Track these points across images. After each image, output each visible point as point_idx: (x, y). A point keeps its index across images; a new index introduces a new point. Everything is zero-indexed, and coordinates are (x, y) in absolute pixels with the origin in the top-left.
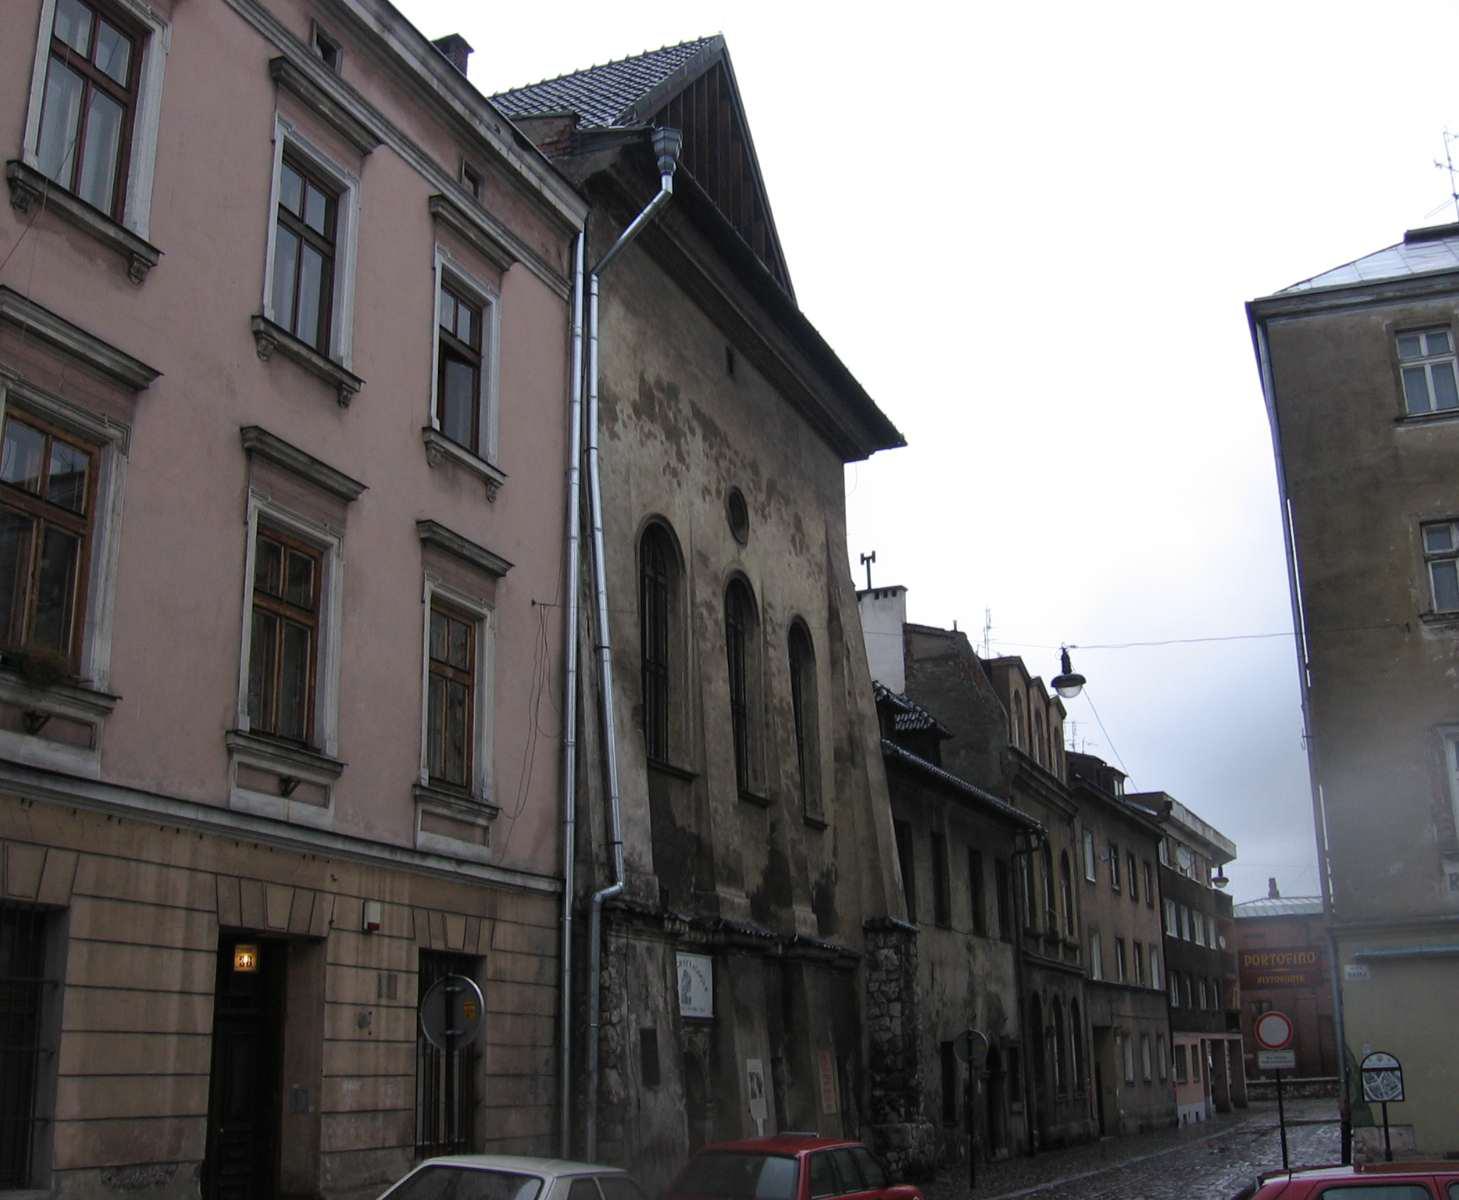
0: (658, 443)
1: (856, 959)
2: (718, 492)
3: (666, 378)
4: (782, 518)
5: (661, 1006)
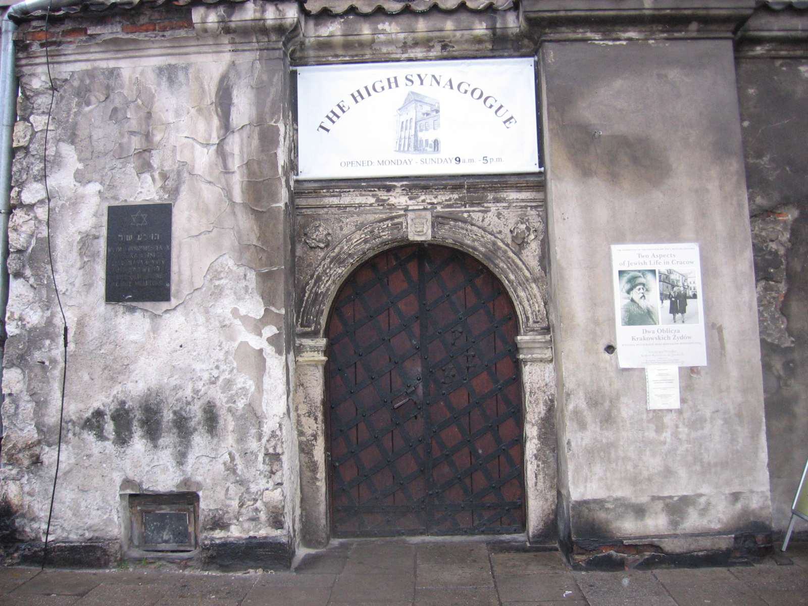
5: (203, 159)
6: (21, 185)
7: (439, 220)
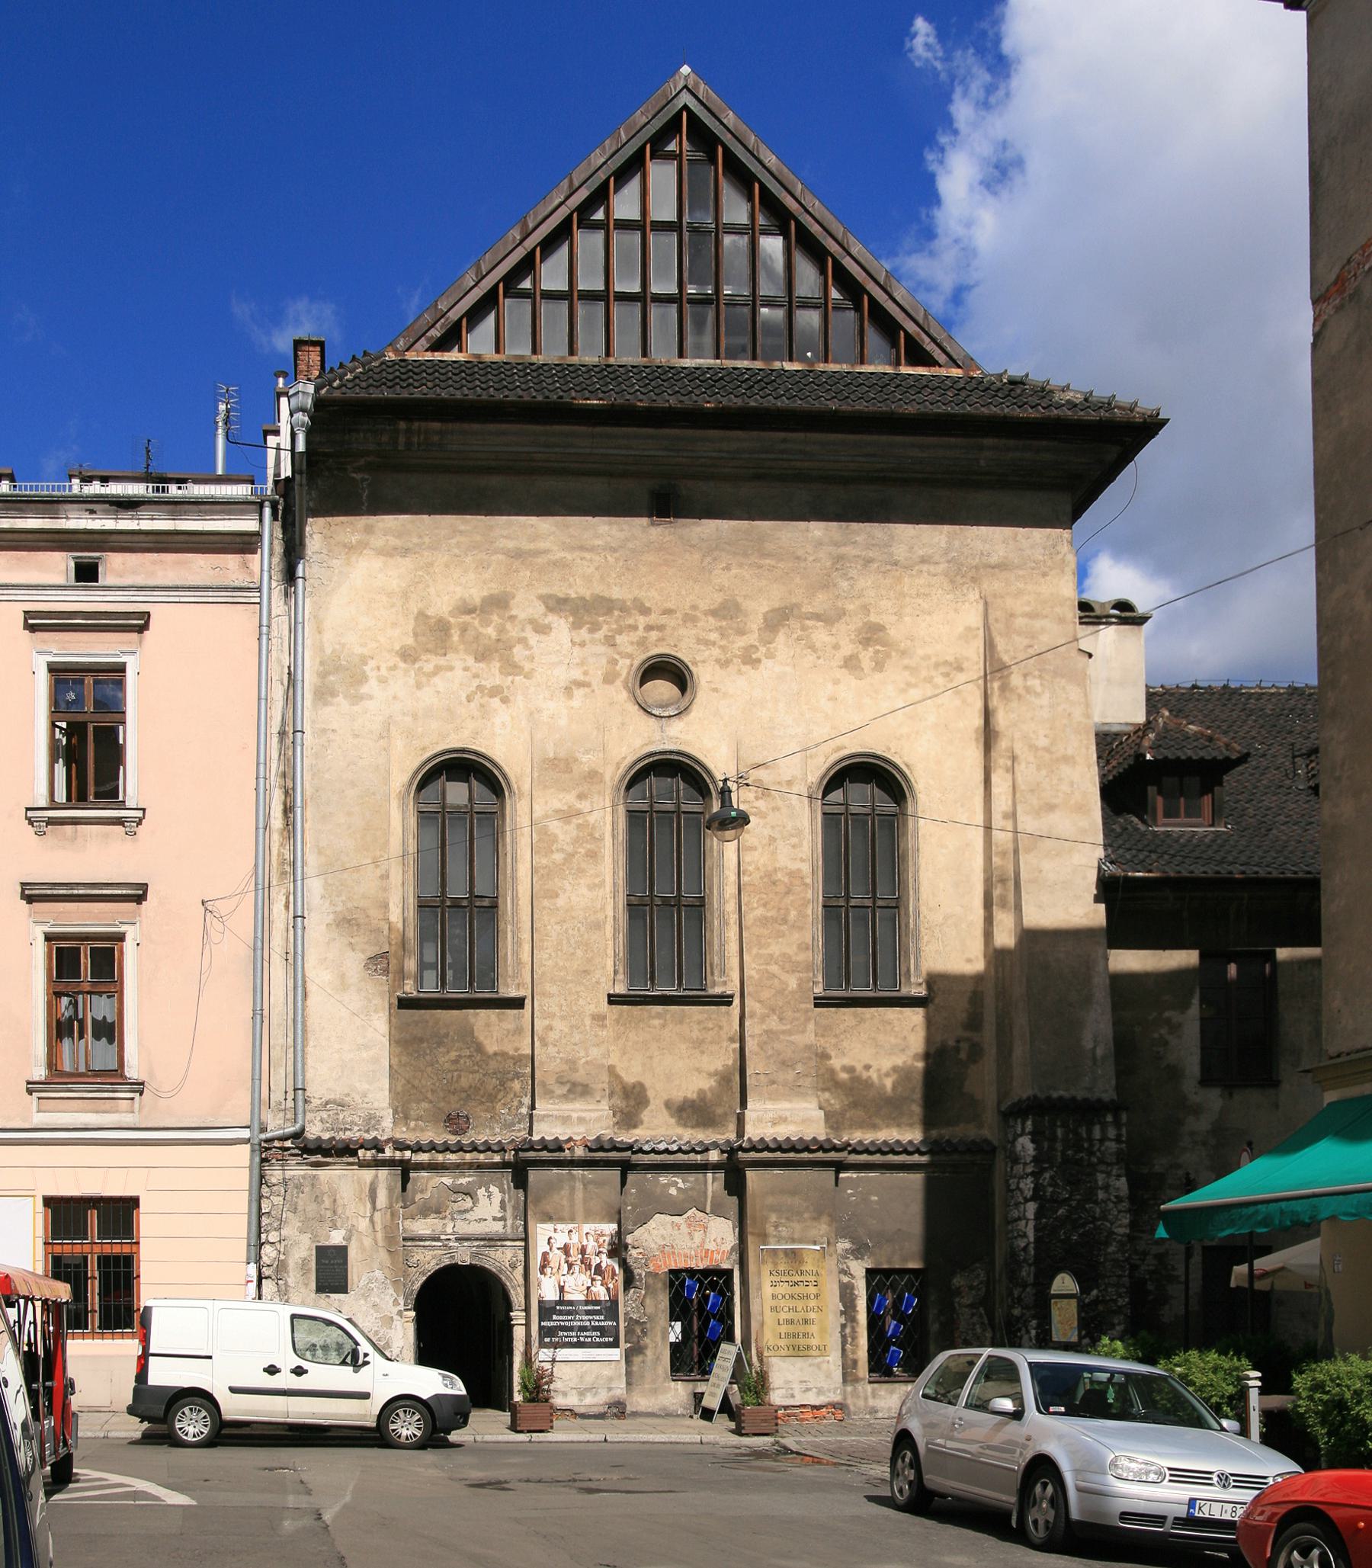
0: (459, 673)
1: (994, 1150)
2: (609, 679)
3: (476, 594)
4: (813, 648)
5: (363, 1224)
6: (267, 1232)
7: (473, 1255)
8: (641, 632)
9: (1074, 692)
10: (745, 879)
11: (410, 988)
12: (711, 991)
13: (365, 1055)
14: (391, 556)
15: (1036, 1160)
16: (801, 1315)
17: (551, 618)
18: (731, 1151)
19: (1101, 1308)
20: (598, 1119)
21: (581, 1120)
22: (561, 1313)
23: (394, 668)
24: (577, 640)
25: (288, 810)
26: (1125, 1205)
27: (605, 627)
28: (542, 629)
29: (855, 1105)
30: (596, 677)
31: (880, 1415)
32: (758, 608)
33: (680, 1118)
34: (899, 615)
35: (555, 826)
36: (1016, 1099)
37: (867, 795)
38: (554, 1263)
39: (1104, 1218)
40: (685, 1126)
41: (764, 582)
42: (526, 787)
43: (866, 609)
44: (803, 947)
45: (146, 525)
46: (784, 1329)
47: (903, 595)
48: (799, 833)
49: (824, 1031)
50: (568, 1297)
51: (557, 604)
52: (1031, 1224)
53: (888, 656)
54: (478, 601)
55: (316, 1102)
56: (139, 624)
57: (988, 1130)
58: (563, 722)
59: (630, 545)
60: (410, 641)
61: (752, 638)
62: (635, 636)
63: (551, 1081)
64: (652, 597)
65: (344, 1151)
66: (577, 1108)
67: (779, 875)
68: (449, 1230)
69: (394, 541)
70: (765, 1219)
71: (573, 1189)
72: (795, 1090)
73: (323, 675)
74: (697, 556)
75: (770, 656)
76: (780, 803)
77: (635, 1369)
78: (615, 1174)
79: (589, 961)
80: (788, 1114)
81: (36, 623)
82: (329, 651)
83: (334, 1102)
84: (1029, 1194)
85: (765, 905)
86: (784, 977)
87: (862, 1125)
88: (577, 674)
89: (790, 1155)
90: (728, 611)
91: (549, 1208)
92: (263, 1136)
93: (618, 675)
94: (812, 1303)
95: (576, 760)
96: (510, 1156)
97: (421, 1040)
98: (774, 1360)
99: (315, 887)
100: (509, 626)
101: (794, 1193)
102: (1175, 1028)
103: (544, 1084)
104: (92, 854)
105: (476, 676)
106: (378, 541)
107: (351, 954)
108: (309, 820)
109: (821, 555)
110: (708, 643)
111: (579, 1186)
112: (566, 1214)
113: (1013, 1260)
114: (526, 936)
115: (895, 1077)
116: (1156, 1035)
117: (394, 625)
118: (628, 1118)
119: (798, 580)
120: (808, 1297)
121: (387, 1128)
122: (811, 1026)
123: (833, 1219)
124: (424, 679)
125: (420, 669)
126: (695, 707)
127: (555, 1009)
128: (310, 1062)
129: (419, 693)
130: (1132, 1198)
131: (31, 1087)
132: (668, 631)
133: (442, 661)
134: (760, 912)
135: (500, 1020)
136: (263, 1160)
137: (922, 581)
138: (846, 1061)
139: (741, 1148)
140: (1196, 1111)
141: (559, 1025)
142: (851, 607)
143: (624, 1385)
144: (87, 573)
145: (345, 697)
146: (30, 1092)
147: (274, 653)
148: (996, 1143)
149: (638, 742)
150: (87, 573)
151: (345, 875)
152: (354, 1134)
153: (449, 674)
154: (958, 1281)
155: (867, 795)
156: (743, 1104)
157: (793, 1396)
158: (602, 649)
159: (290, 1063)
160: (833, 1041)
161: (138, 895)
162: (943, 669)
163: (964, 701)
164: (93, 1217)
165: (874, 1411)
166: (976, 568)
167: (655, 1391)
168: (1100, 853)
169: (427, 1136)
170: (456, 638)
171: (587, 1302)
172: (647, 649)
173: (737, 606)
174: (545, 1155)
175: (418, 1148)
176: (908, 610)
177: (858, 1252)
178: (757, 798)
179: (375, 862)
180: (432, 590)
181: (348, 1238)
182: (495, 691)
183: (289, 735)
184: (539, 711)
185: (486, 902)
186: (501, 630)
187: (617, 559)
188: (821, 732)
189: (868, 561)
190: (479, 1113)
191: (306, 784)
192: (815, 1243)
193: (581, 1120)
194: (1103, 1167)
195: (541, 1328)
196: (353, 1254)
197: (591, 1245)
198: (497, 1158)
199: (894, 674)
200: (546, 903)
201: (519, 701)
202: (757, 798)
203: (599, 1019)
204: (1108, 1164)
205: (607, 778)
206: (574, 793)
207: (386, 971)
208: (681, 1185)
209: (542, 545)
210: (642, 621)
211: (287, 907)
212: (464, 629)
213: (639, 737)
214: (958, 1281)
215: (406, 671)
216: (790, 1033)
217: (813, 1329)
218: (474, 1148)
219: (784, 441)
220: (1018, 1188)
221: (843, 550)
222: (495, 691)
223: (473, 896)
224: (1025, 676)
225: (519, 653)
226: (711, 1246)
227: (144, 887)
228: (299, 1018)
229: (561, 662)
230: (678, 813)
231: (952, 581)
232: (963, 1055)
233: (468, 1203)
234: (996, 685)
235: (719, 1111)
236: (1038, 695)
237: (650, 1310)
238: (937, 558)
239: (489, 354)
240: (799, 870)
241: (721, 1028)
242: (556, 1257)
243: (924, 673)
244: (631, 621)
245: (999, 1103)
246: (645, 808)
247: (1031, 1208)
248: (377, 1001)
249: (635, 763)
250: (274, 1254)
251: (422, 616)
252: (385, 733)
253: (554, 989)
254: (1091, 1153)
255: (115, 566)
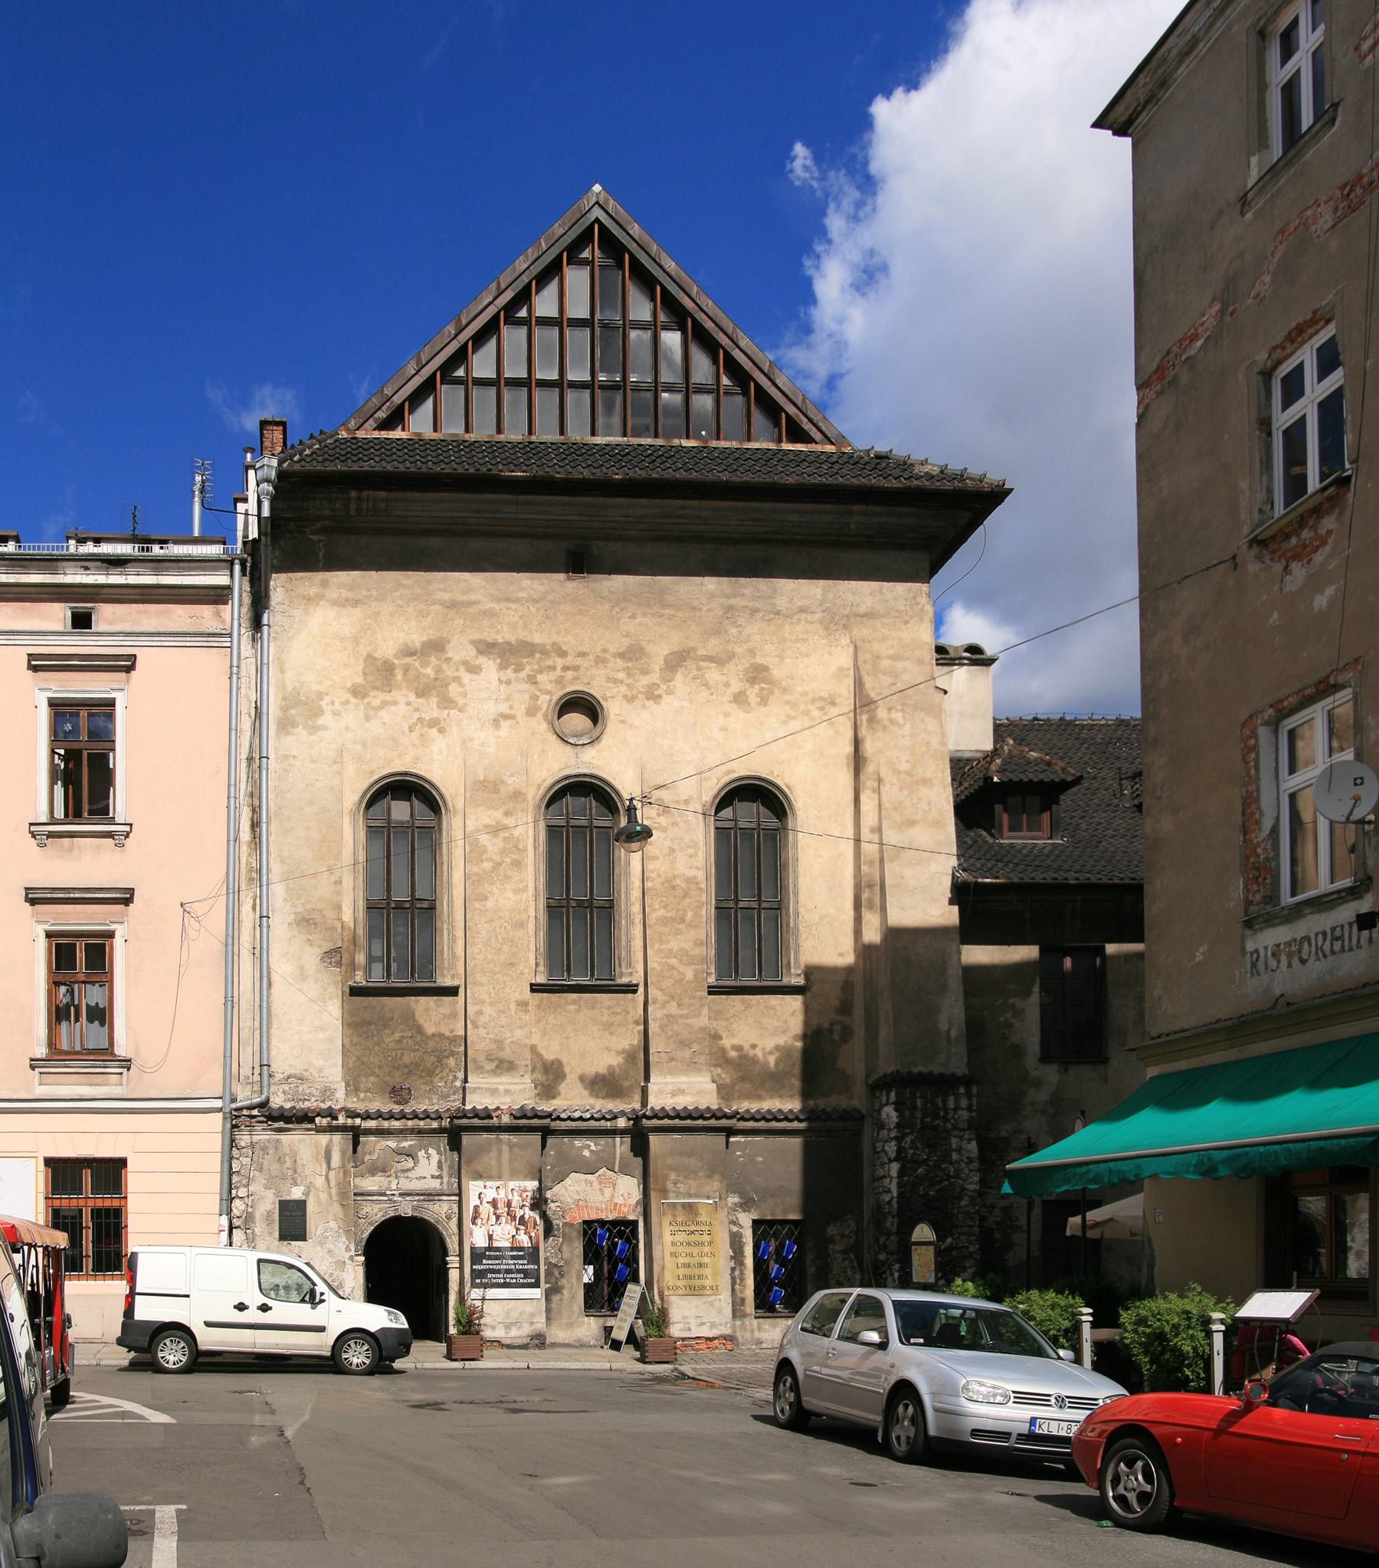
0: (402, 707)
1: (862, 1118)
2: (531, 712)
3: (417, 639)
4: (706, 685)
5: (320, 1181)
7: (414, 1208)
8: (559, 672)
9: (931, 724)
10: (648, 884)
11: (359, 978)
12: (619, 981)
13: (321, 1036)
14: (344, 606)
15: (898, 1126)
16: (697, 1259)
17: (482, 660)
18: (636, 1119)
19: (954, 1253)
20: (522, 1091)
21: (507, 1092)
22: (490, 1258)
23: (346, 703)
24: (504, 679)
25: (255, 825)
26: (976, 1165)
27: (528, 668)
28: (474, 670)
29: (743, 1079)
30: (520, 710)
31: (764, 1345)
32: (659, 652)
33: (592, 1090)
34: (781, 657)
35: (484, 839)
36: (882, 1073)
37: (754, 813)
38: (484, 1215)
39: (957, 1176)
40: (597, 1097)
41: (665, 629)
42: (460, 804)
43: (752, 652)
44: (698, 943)
45: (133, 580)
46: (682, 1272)
47: (784, 640)
48: (694, 845)
49: (716, 1015)
50: (496, 1244)
51: (486, 648)
52: (895, 1181)
53: (772, 692)
54: (418, 645)
55: (279, 1077)
56: (126, 665)
57: (857, 1100)
58: (491, 750)
59: (550, 597)
60: (360, 679)
61: (655, 677)
62: (553, 675)
63: (481, 1058)
64: (568, 642)
65: (302, 1118)
66: (503, 1081)
67: (678, 882)
68: (394, 1187)
69: (345, 594)
70: (666, 1177)
71: (500, 1151)
72: (691, 1066)
73: (285, 709)
74: (607, 607)
75: (670, 692)
76: (678, 819)
77: (553, 1306)
78: (536, 1138)
79: (514, 954)
80: (685, 1086)
81: (38, 664)
82: (290, 688)
83: (295, 1076)
84: (893, 1155)
85: (665, 907)
86: (682, 968)
87: (748, 1096)
88: (504, 708)
89: (687, 1122)
90: (634, 654)
91: (479, 1168)
92: (234, 1106)
93: (537, 709)
94: (706, 1249)
95: (503, 782)
96: (446, 1123)
97: (370, 1023)
98: (673, 1299)
99: (278, 891)
100: (445, 667)
101: (690, 1154)
102: (1018, 1013)
103: (475, 1061)
104: (86, 863)
105: (417, 710)
106: (332, 594)
107: (308, 948)
108: (272, 833)
109: (714, 605)
110: (616, 681)
111: (505, 1148)
112: (494, 1173)
113: (879, 1211)
114: (460, 933)
115: (777, 1054)
116: (1002, 1019)
117: (346, 666)
118: (548, 1091)
119: (694, 627)
120: (703, 1244)
121: (340, 1099)
122: (705, 1011)
123: (724, 1177)
124: (372, 713)
125: (369, 703)
126: (605, 736)
127: (484, 996)
128: (273, 1042)
129: (368, 725)
130: (982, 1159)
131: (34, 1064)
132: (582, 670)
133: (388, 697)
134: (661, 913)
135: (438, 1006)
136: (234, 1126)
137: (800, 628)
138: (735, 1041)
139: (644, 1116)
140: (1037, 1084)
141: (489, 1010)
142: (739, 650)
143: (544, 1320)
144: (82, 621)
145: (304, 728)
146: (33, 1068)
147: (243, 690)
148: (864, 1112)
149: (556, 767)
150: (82, 621)
151: (304, 881)
152: (311, 1104)
153: (393, 708)
154: (831, 1230)
155: (754, 813)
156: (647, 1078)
157: (689, 1329)
158: (526, 686)
159: (257, 1043)
160: (724, 1024)
161: (126, 898)
162: (818, 704)
163: (837, 732)
164: (87, 1176)
165: (759, 1342)
166: (848, 617)
167: (570, 1325)
168: (954, 862)
169: (374, 1106)
170: (399, 677)
171: (512, 1249)
172: (564, 687)
173: (642, 649)
174: (476, 1122)
175: (367, 1116)
176: (789, 653)
177: (746, 1205)
178: (658, 815)
179: (330, 870)
180: (379, 636)
181: (307, 1194)
182: (433, 723)
183: (256, 760)
184: (471, 740)
185: (425, 905)
186: (439, 670)
187: (538, 609)
188: (714, 758)
189: (755, 611)
190: (419, 1085)
191: (271, 802)
192: (708, 1198)
193: (507, 1092)
194: (956, 1133)
195: (473, 1271)
196: (310, 1207)
197: (516, 1200)
198: (435, 1125)
199: (776, 709)
200: (477, 905)
201: (454, 731)
202: (658, 815)
203: (523, 1005)
204: (961, 1130)
205: (530, 797)
206: (501, 810)
207: (339, 964)
208: (593, 1148)
209: (474, 597)
210: (559, 662)
211: (254, 908)
212: (406, 669)
213: (558, 762)
214: (831, 1230)
215: (357, 705)
216: (686, 1017)
217: (707, 1271)
218: (415, 1116)
219: (682, 507)
220: (883, 1150)
221: (733, 601)
222: (433, 723)
223: (414, 899)
224: (889, 709)
225: (454, 690)
226: (619, 1200)
227: (131, 891)
228: (265, 1004)
229: (490, 698)
230: (591, 827)
231: (826, 628)
232: (836, 1036)
233: (410, 1163)
234: (864, 717)
235: (626, 1084)
236: (900, 726)
237: (566, 1255)
238: (813, 608)
239: (428, 433)
240: (695, 877)
241: (627, 1012)
242: (486, 1209)
243: (802, 707)
244: (550, 663)
245: (867, 1077)
246: (563, 823)
247: (895, 1168)
248: (332, 989)
249: (554, 785)
250: (243, 1207)
251: (370, 658)
252: (338, 760)
253: (484, 979)
254: (946, 1120)
255: (106, 615)
